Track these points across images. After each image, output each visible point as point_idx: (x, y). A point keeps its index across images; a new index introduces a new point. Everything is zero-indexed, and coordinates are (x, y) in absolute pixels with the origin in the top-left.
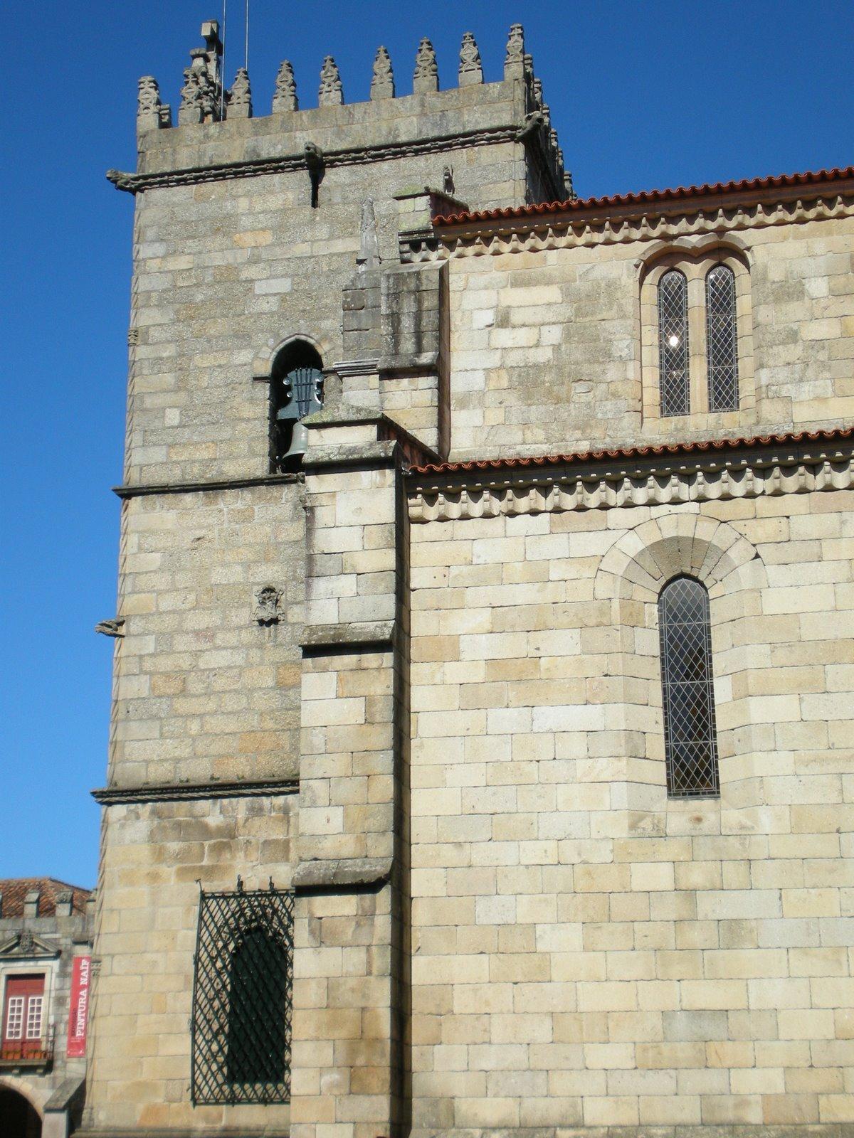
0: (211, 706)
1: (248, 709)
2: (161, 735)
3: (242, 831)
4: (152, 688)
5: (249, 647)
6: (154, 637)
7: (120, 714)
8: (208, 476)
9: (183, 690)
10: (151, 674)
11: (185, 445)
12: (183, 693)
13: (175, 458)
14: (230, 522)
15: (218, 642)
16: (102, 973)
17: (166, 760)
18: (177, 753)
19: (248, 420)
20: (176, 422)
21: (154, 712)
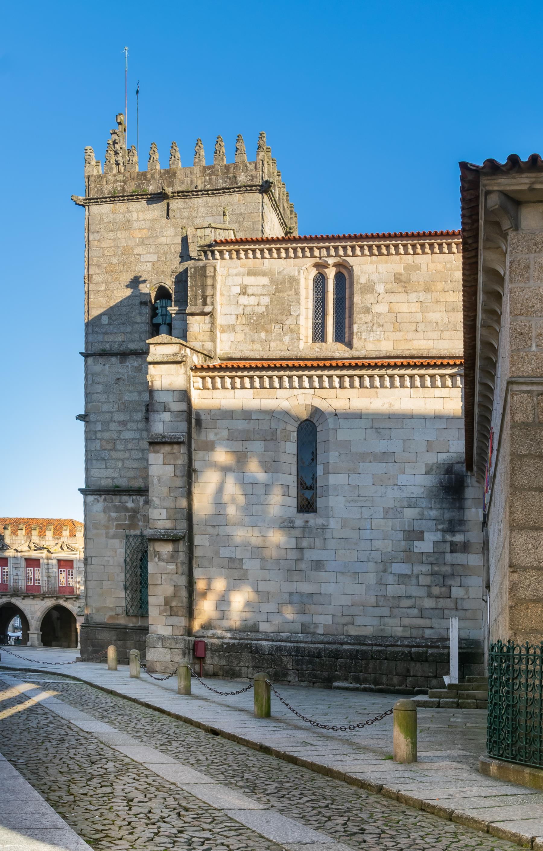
2: (106, 467)
3: (141, 510)
4: (101, 446)
5: (142, 430)
8: (121, 349)
9: (114, 448)
10: (101, 440)
11: (111, 334)
12: (114, 449)
13: (106, 340)
14: (132, 372)
15: (129, 427)
17: (109, 478)
18: (113, 475)
19: (139, 323)
20: (106, 322)
21: (103, 456)
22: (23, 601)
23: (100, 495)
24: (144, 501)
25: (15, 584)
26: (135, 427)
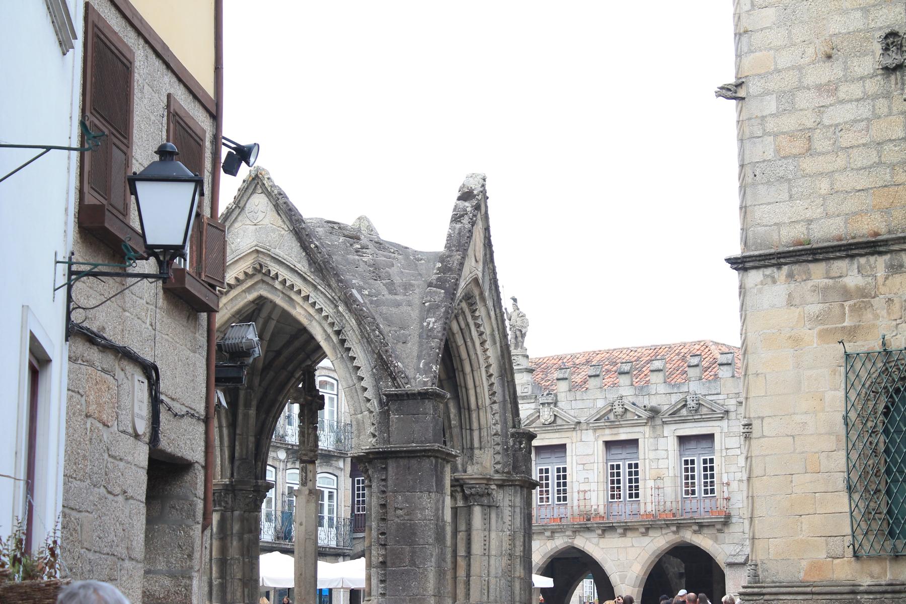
0: (841, 162)
1: (880, 163)
3: (882, 289)
4: (777, 151)
5: (875, 97)
6: (774, 96)
7: (747, 178)
10: (776, 135)
12: (809, 151)
15: (842, 95)
16: (754, 435)
18: (809, 214)
22: (602, 540)
23: (779, 266)
24: (886, 267)
25: (582, 503)
26: (859, 93)
